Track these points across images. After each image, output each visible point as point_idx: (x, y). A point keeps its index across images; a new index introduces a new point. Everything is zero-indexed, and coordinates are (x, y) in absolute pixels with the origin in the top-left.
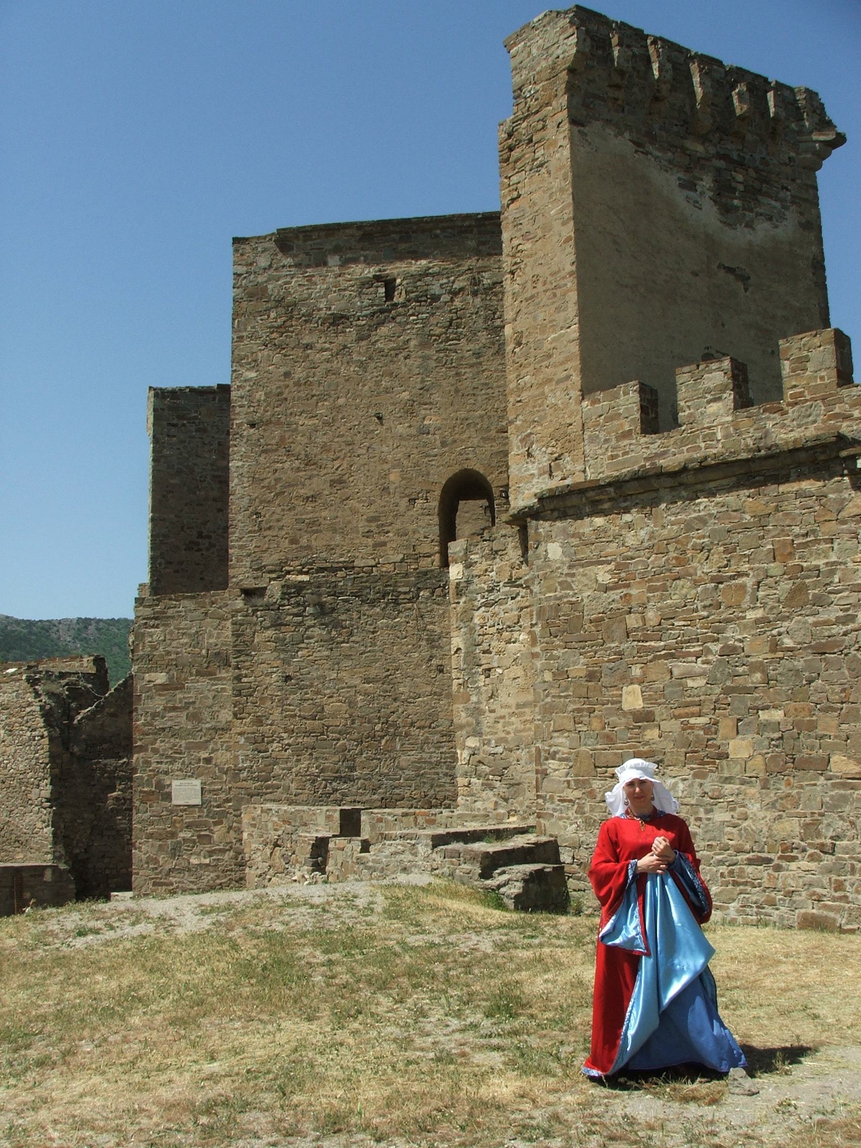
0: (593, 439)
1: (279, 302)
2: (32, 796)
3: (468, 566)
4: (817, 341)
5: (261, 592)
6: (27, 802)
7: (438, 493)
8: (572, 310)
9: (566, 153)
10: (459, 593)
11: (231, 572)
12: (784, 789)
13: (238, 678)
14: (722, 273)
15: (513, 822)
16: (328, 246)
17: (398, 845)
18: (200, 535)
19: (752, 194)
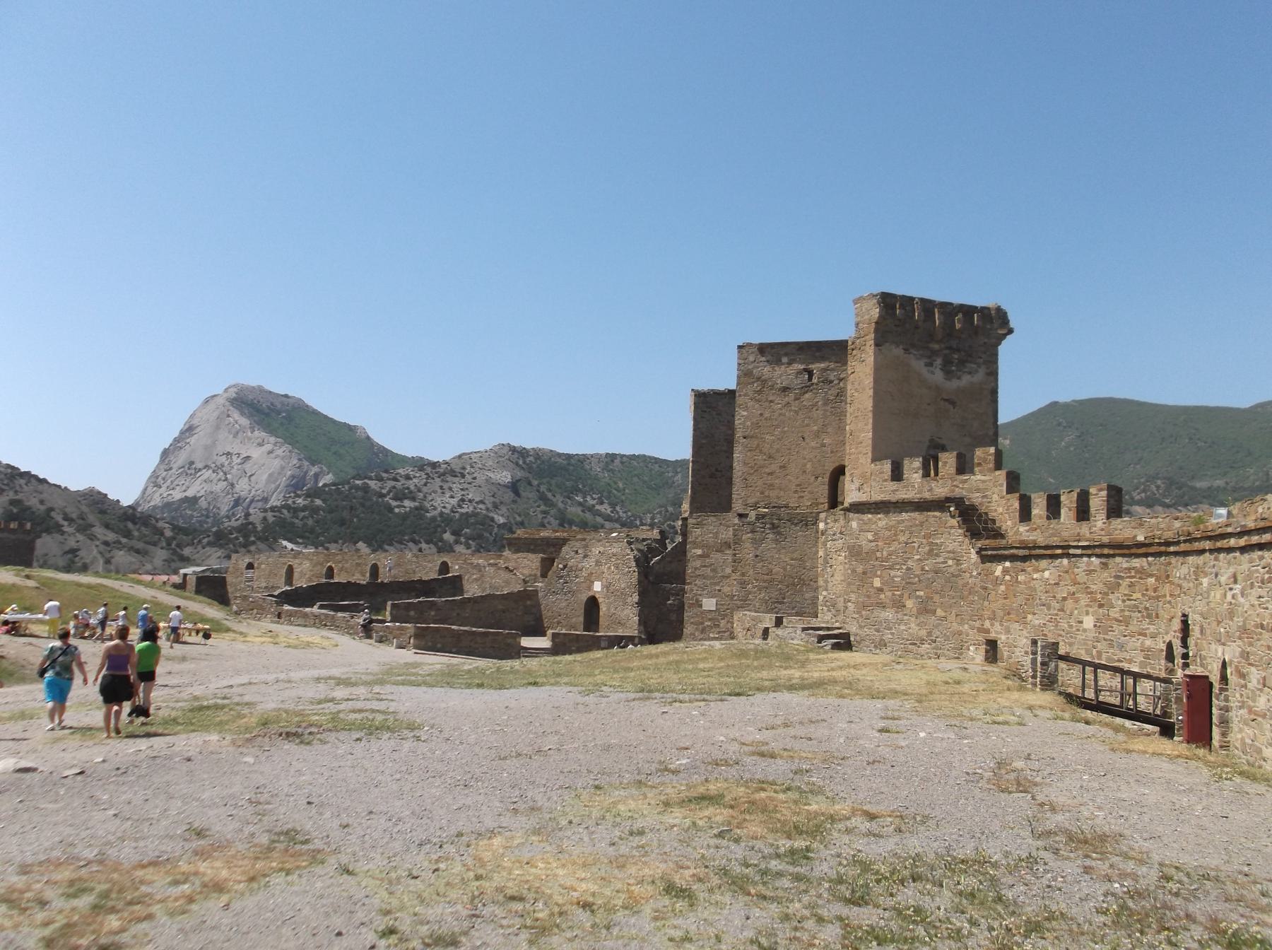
0: (874, 480)
1: (759, 379)
2: (628, 601)
3: (827, 524)
4: (951, 456)
5: (746, 516)
6: (625, 603)
7: (828, 475)
8: (870, 426)
9: (872, 359)
10: (823, 534)
11: (733, 506)
12: (922, 620)
13: (735, 555)
14: (942, 402)
15: (837, 625)
16: (782, 352)
17: (790, 630)
18: (717, 470)
19: (962, 363)
